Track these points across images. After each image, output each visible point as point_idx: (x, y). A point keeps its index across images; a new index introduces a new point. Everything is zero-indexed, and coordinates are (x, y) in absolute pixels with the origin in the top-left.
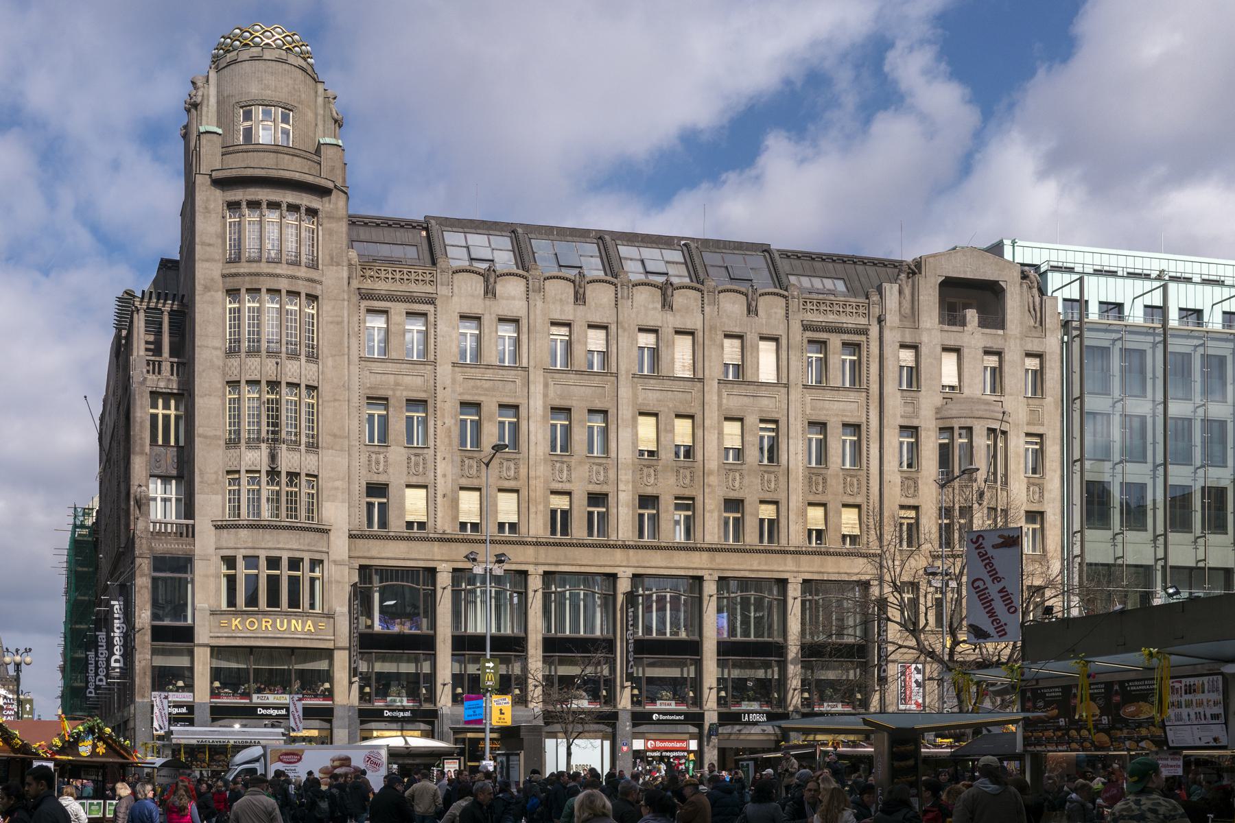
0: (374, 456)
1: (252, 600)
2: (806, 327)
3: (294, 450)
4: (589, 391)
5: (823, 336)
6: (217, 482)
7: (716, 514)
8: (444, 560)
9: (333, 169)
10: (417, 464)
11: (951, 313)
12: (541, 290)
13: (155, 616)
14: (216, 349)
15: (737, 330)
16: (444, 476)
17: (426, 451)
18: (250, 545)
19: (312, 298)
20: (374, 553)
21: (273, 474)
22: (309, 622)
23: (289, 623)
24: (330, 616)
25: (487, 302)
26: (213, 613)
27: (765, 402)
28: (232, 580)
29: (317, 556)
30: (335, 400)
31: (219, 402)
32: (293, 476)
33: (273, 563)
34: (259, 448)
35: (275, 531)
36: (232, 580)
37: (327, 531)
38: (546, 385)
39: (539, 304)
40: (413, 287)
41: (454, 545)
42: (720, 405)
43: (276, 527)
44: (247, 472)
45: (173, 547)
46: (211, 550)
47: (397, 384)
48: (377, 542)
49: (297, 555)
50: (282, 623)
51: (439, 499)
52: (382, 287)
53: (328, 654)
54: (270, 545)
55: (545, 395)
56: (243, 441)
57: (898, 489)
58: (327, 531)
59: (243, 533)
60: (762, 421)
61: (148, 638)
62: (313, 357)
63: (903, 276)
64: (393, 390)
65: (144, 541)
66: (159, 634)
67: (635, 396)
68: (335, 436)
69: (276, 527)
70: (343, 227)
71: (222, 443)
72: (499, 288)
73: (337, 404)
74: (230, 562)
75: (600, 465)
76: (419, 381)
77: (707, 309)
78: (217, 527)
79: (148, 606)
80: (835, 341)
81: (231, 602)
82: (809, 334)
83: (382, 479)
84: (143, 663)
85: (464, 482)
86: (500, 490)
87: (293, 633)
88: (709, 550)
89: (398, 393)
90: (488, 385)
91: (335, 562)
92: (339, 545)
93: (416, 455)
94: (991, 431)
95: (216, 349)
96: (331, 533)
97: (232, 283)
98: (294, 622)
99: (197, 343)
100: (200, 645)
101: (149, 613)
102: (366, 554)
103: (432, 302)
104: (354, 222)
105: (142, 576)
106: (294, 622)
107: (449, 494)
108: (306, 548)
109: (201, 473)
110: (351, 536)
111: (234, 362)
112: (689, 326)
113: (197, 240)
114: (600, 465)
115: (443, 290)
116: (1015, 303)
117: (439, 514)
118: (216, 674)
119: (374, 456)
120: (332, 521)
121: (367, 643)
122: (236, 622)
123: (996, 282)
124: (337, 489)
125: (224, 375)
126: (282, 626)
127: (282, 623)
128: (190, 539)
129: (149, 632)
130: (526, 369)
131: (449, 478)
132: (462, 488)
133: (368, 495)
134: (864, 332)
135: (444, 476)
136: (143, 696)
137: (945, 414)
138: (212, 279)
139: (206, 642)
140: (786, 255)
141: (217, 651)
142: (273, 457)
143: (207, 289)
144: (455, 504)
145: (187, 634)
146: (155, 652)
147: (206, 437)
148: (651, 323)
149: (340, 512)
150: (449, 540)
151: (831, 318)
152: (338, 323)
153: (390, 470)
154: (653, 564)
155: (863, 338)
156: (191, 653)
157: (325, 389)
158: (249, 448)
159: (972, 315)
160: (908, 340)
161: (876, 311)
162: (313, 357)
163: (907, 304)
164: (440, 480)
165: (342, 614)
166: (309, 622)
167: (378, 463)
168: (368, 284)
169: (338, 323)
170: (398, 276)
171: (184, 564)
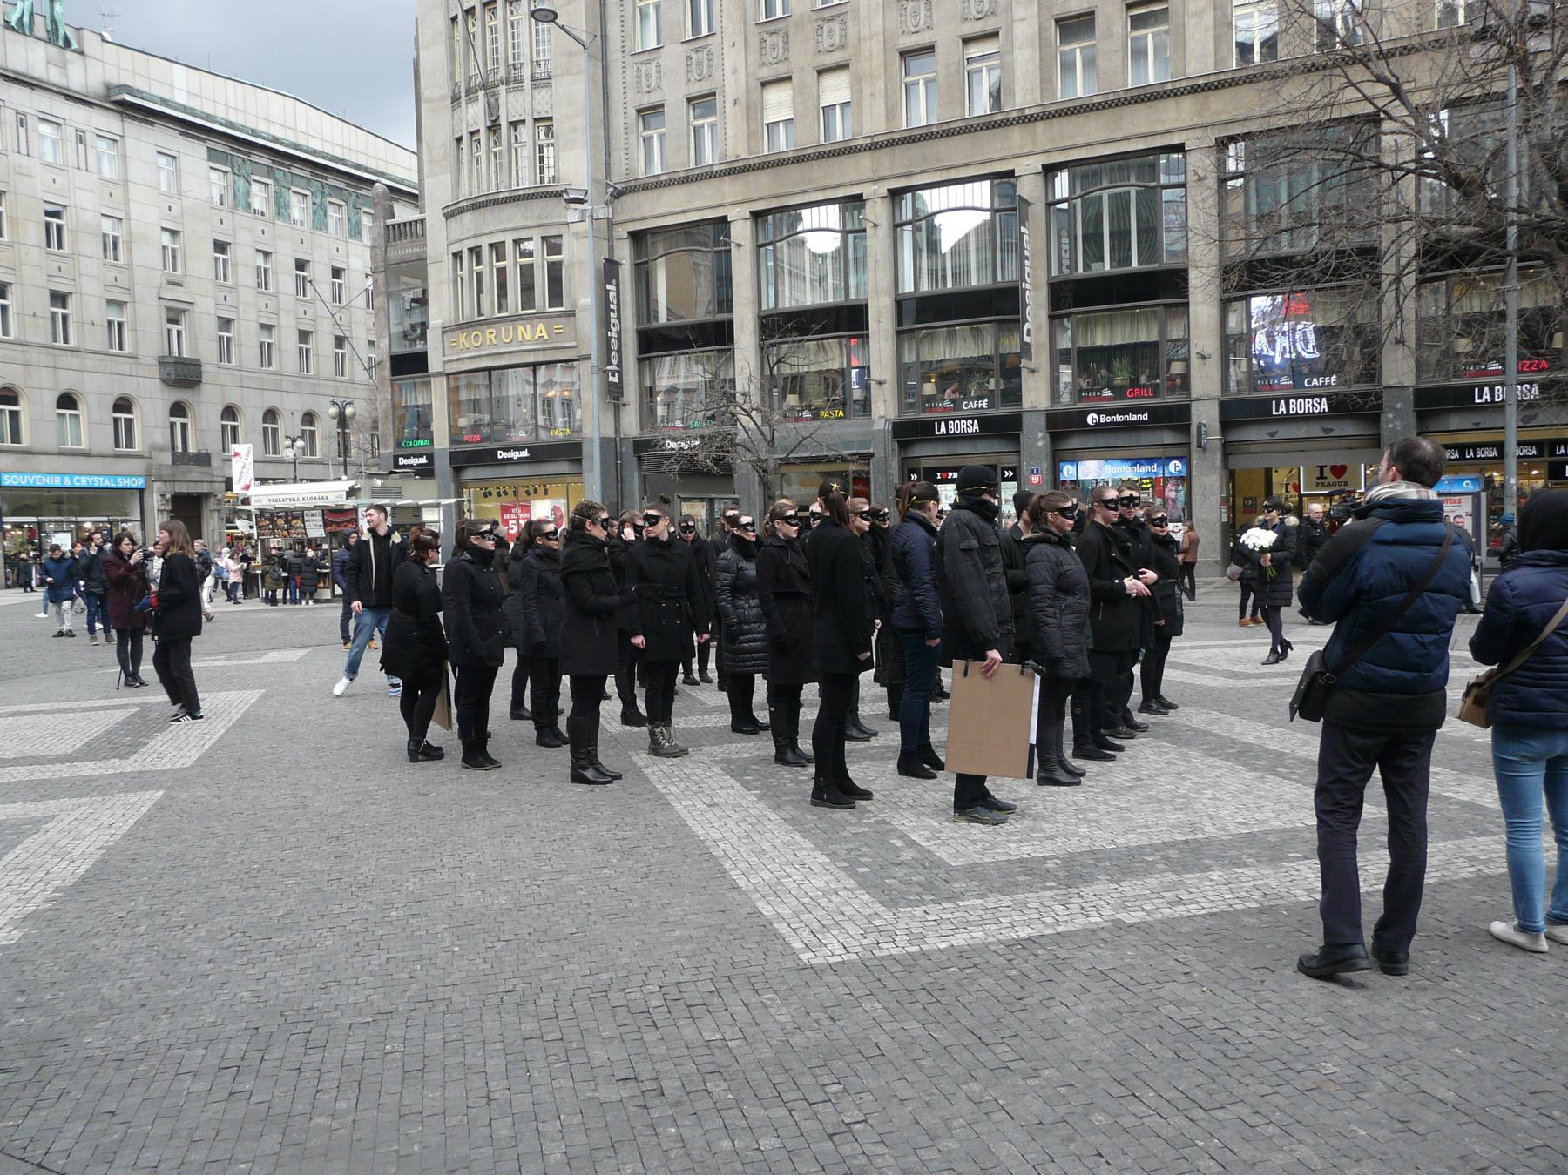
0: (643, 68)
3: (517, 89)
8: (733, 202)
10: (699, 64)
17: (710, 40)
20: (646, 212)
22: (541, 326)
23: (515, 330)
33: (498, 249)
35: (496, 208)
41: (751, 176)
48: (649, 194)
50: (507, 331)
54: (492, 228)
83: (653, 99)
85: (766, 73)
93: (697, 51)
98: (521, 328)
102: (637, 215)
106: (521, 328)
107: (743, 99)
108: (535, 222)
124: (575, 130)
127: (507, 331)
129: (388, 365)
135: (735, 71)
153: (664, 84)
154: (1081, 140)
156: (429, 384)
165: (585, 308)
166: (541, 326)
167: (648, 76)
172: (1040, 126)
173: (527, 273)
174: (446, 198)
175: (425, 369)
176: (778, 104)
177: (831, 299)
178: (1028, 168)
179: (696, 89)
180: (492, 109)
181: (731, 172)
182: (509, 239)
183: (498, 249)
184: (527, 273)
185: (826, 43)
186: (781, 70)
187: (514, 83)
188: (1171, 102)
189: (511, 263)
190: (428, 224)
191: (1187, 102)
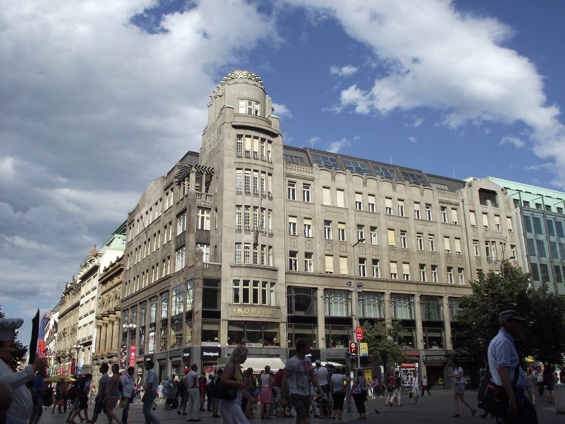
0: (292, 240)
1: (246, 299)
2: (440, 202)
4: (370, 219)
5: (445, 205)
6: (232, 247)
7: (417, 270)
8: (321, 285)
9: (276, 127)
10: (309, 244)
11: (483, 201)
12: (351, 180)
13: (204, 306)
14: (232, 191)
15: (418, 201)
16: (320, 249)
18: (246, 275)
19: (270, 175)
20: (293, 281)
21: (256, 245)
23: (263, 310)
24: (278, 308)
25: (333, 182)
26: (230, 305)
27: (429, 228)
28: (236, 290)
29: (273, 281)
32: (263, 246)
34: (250, 234)
36: (236, 290)
37: (277, 271)
38: (355, 216)
39: (351, 185)
40: (305, 174)
42: (415, 228)
43: (258, 268)
44: (245, 243)
45: (211, 275)
47: (300, 211)
49: (266, 280)
51: (318, 259)
52: (294, 173)
53: (277, 325)
55: (355, 220)
57: (475, 263)
58: (277, 271)
59: (244, 270)
60: (429, 235)
61: (200, 316)
62: (271, 199)
63: (467, 186)
64: (299, 213)
65: (200, 272)
66: (205, 314)
67: (386, 223)
68: (279, 231)
69: (258, 268)
70: (281, 149)
71: (234, 230)
72: (336, 177)
74: (236, 282)
75: (376, 248)
76: (308, 211)
77: (408, 192)
79: (201, 302)
80: (449, 207)
81: (236, 298)
82: (441, 204)
84: (198, 328)
85: (327, 253)
86: (341, 256)
88: (417, 284)
89: (301, 215)
90: (334, 214)
92: (281, 277)
93: (309, 240)
94: (501, 243)
95: (232, 191)
97: (239, 166)
99: (225, 188)
100: (223, 320)
101: (201, 304)
103: (313, 180)
104: (285, 147)
109: (225, 243)
110: (286, 273)
111: (239, 197)
112: (402, 198)
114: (376, 248)
115: (316, 177)
116: (500, 198)
117: (318, 265)
118: (230, 334)
119: (292, 240)
121: (292, 320)
122: (240, 310)
123: (495, 191)
130: (347, 209)
131: (322, 250)
132: (326, 255)
133: (290, 256)
134: (458, 205)
136: (198, 344)
137: (486, 236)
139: (226, 318)
140: (429, 175)
141: (231, 323)
142: (256, 238)
143: (229, 167)
144: (324, 261)
145: (217, 315)
146: (203, 323)
147: (227, 228)
148: (389, 196)
149: (281, 263)
150: (323, 276)
151: (447, 199)
152: (280, 185)
155: (457, 207)
156: (219, 323)
157: (275, 210)
158: (246, 233)
159: (489, 202)
160: (472, 209)
161: (461, 198)
162: (271, 199)
163: (470, 197)
164: (318, 252)
165: (283, 307)
167: (294, 243)
168: (289, 171)
169: (280, 185)
170: (299, 169)
171: (217, 282)
172: (390, 284)
173: (255, 291)
174: (232, 261)
175: (219, 317)
176: (329, 261)
177: (345, 315)
178: (388, 293)
179: (308, 251)
180: (256, 238)
181: (319, 276)
182: (252, 280)
183: (255, 283)
184: (255, 291)
185: (342, 250)
186: (331, 253)
187: (264, 234)
188: (412, 285)
189: (251, 287)
190: (223, 267)
191: (415, 286)
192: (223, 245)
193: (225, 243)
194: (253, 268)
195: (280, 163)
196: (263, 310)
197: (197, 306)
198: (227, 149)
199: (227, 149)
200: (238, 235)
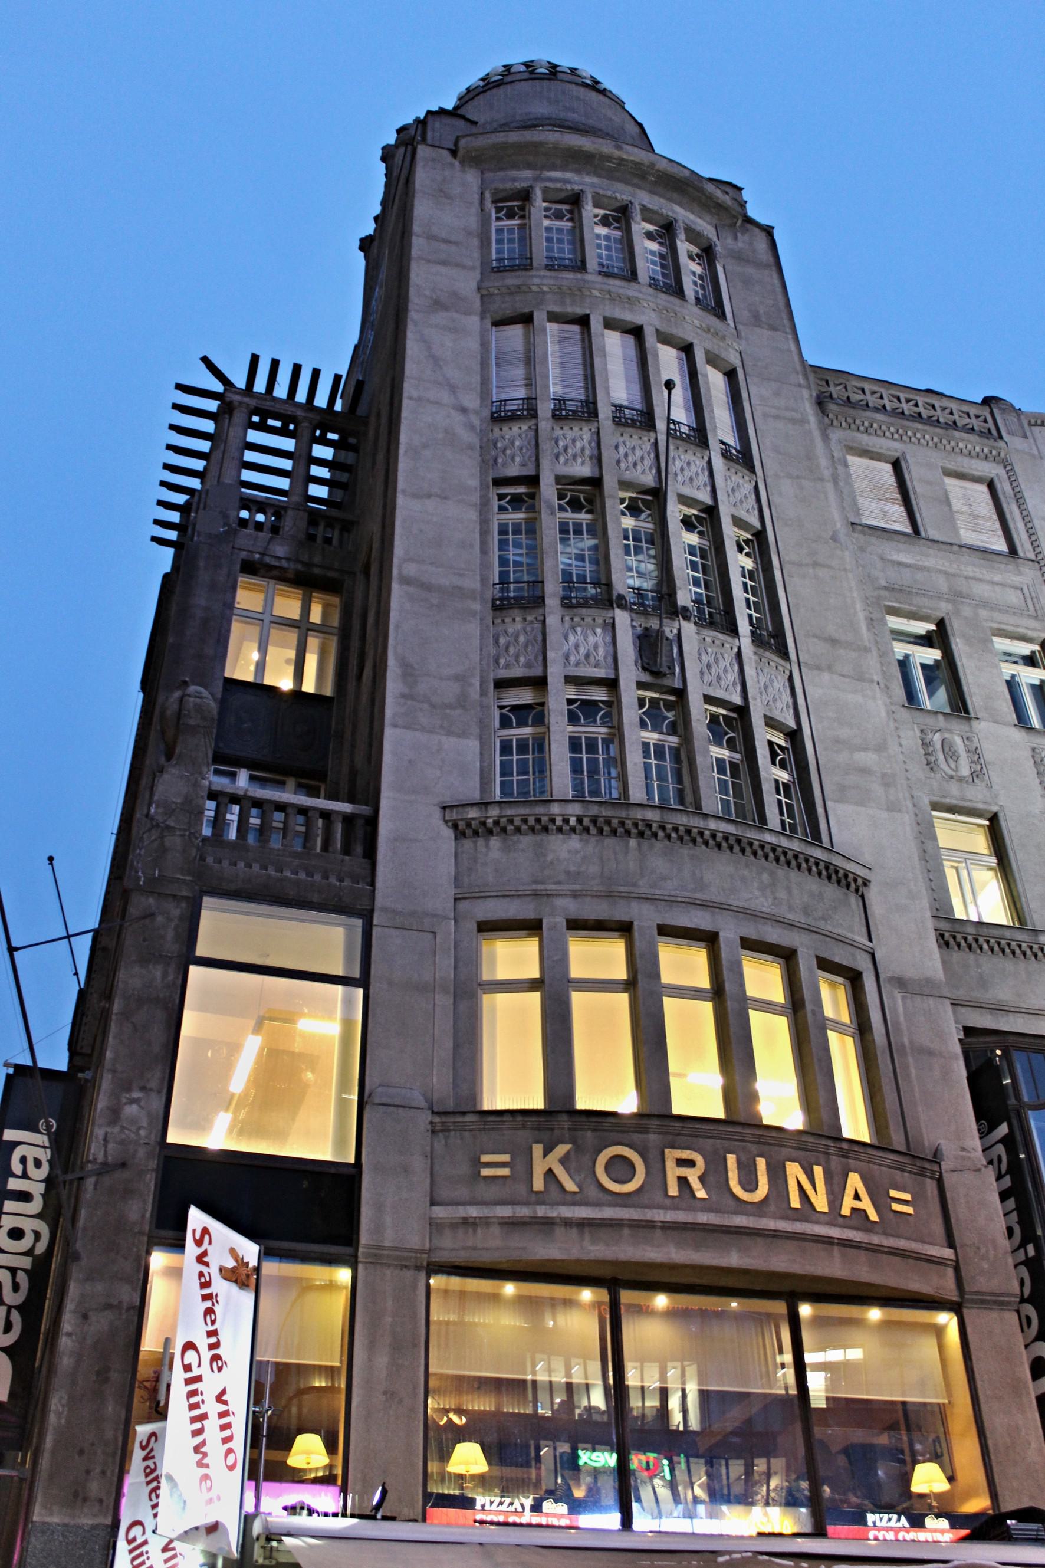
6: (462, 702)
20: (1003, 993)
22: (854, 1181)
23: (777, 1175)
30: (816, 564)
31: (473, 515)
44: (570, 680)
46: (441, 901)
48: (1008, 964)
56: (552, 602)
68: (833, 642)
73: (821, 572)
78: (461, 831)
87: (796, 1215)
91: (900, 983)
96: (873, 895)
98: (794, 1170)
105: (144, 960)
106: (794, 1170)
113: (416, 228)
120: (867, 858)
122: (543, 1163)
124: (864, 771)
125: (488, 461)
126: (750, 1184)
128: (355, 863)
138: (455, 294)
166: (854, 1181)
167: (951, 754)
192: (393, 686)
193: (409, 673)
194: (645, 832)
195: (773, 328)
196: (777, 1175)
197: (115, 1114)
198: (431, 237)
199: (431, 237)
200: (516, 624)
